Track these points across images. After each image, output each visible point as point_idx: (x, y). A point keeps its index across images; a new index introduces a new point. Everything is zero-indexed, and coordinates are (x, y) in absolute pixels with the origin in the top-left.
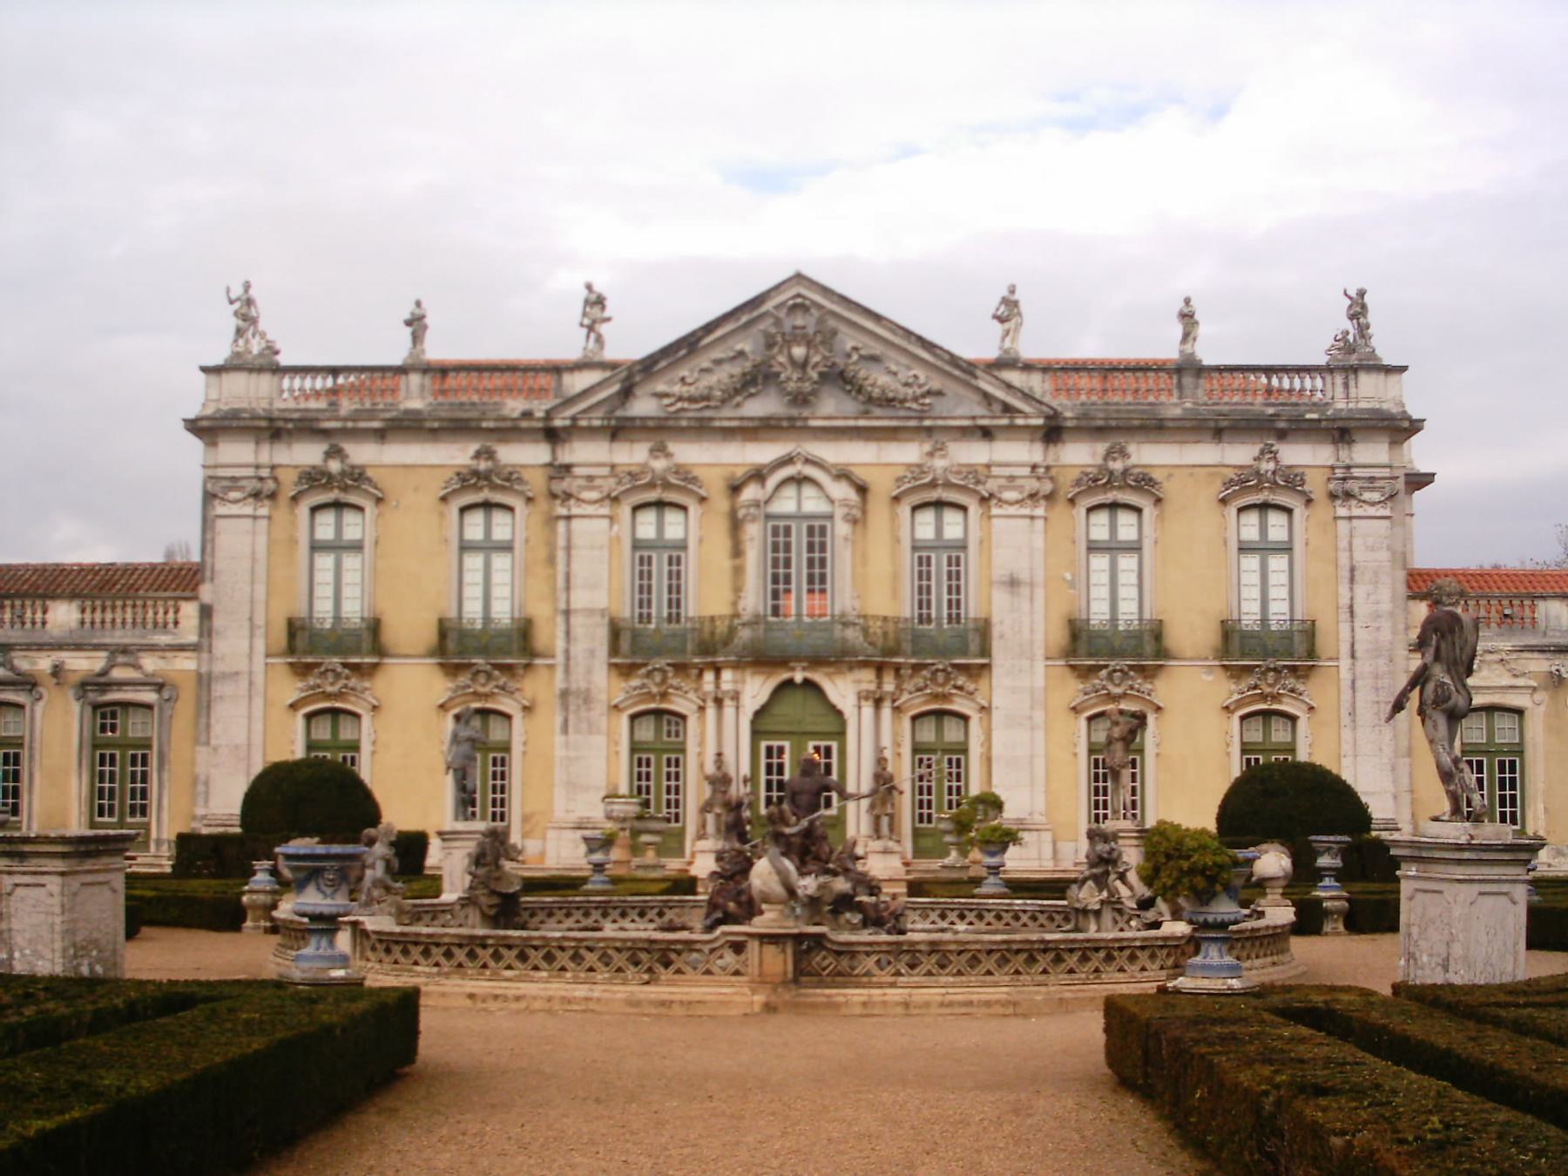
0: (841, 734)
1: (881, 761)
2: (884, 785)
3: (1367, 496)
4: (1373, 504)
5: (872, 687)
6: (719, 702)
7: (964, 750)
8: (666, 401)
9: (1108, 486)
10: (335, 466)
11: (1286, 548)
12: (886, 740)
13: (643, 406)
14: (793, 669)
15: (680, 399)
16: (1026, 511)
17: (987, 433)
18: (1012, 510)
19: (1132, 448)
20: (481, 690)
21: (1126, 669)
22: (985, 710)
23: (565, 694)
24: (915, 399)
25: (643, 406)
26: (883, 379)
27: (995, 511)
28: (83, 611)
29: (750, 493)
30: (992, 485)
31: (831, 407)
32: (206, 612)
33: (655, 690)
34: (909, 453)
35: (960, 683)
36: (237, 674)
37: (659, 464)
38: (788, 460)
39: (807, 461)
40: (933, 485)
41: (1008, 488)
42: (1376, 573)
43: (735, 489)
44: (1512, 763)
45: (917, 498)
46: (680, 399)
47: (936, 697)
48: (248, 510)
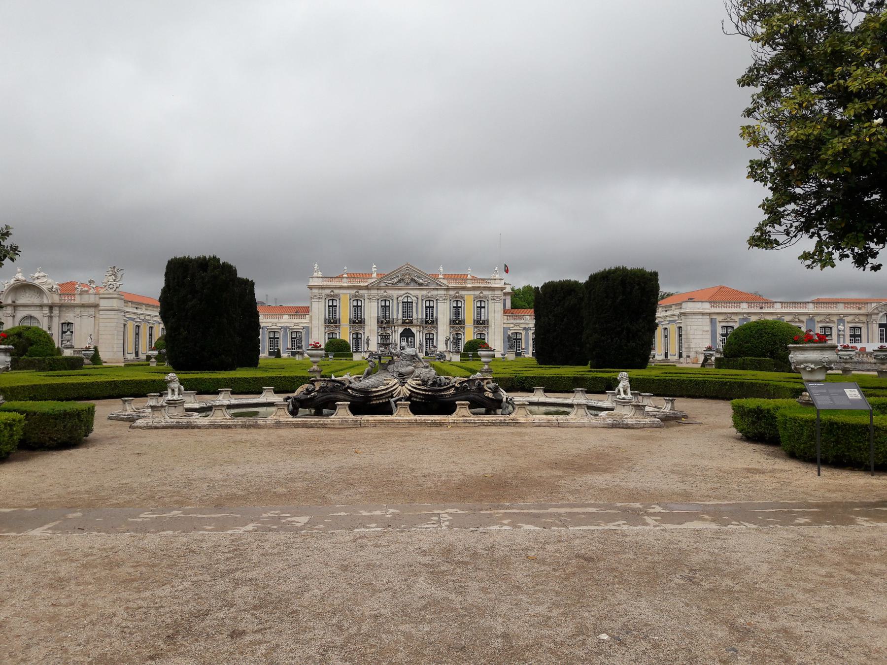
1: (420, 341)
2: (421, 345)
6: (395, 332)
7: (433, 339)
9: (456, 298)
10: (332, 294)
11: (484, 307)
12: (421, 338)
13: (383, 285)
17: (437, 289)
19: (460, 292)
22: (437, 333)
25: (383, 285)
26: (421, 281)
30: (438, 298)
31: (412, 285)
34: (425, 292)
37: (385, 294)
40: (429, 297)
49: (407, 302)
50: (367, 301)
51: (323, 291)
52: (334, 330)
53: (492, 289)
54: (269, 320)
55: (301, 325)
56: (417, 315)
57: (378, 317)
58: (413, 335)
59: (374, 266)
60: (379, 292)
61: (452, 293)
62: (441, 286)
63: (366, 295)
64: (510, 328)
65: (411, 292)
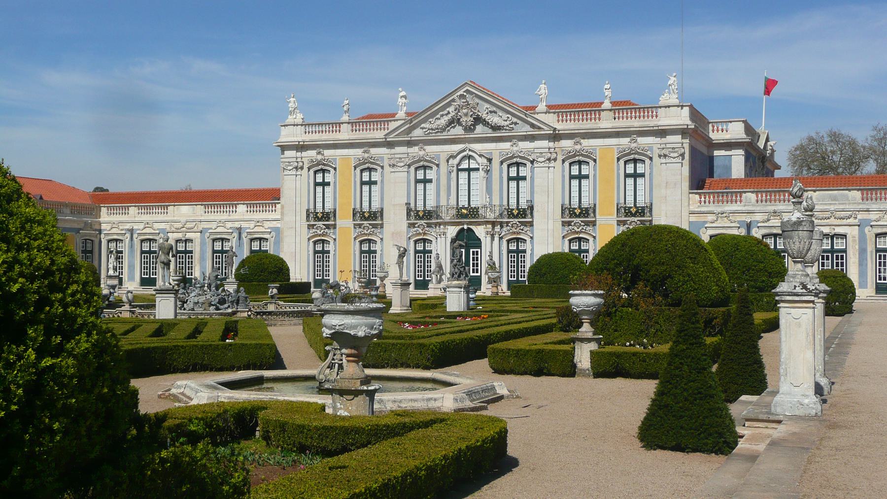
0: (480, 247)
3: (672, 155)
4: (674, 158)
5: (490, 230)
8: (424, 130)
14: (463, 225)
15: (429, 129)
16: (547, 165)
18: (542, 165)
20: (366, 232)
21: (580, 222)
23: (393, 233)
24: (508, 126)
25: (417, 133)
27: (535, 165)
28: (248, 207)
29: (451, 161)
32: (282, 207)
33: (421, 232)
35: (522, 228)
36: (292, 228)
38: (464, 151)
39: (470, 150)
41: (540, 157)
42: (675, 184)
43: (448, 161)
44: (842, 257)
45: (509, 162)
46: (429, 129)
47: (514, 233)
48: (294, 173)
49: (469, 170)
50: (387, 169)
51: (304, 154)
52: (519, 233)
53: (662, 133)
54: (211, 217)
55: (267, 225)
56: (491, 199)
57: (408, 204)
58: (477, 244)
59: (403, 93)
60: (410, 150)
61: (567, 144)
62: (540, 128)
63: (386, 157)
64: (706, 222)
65: (477, 147)
